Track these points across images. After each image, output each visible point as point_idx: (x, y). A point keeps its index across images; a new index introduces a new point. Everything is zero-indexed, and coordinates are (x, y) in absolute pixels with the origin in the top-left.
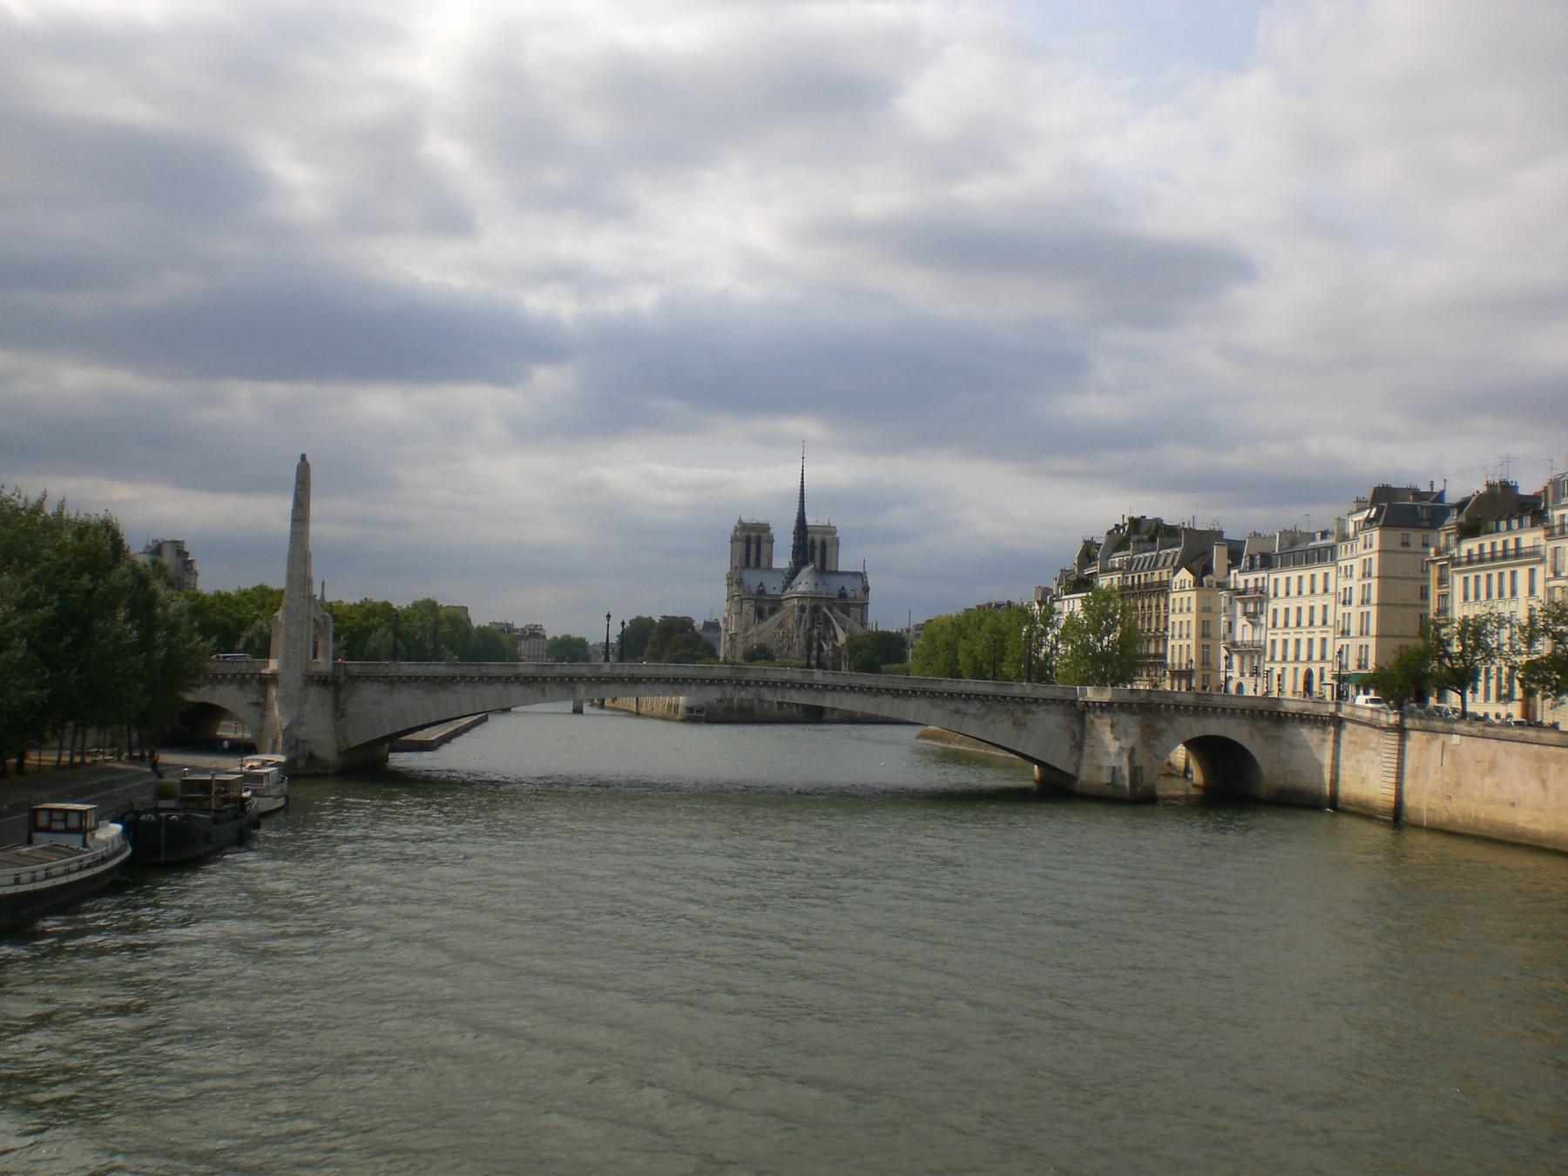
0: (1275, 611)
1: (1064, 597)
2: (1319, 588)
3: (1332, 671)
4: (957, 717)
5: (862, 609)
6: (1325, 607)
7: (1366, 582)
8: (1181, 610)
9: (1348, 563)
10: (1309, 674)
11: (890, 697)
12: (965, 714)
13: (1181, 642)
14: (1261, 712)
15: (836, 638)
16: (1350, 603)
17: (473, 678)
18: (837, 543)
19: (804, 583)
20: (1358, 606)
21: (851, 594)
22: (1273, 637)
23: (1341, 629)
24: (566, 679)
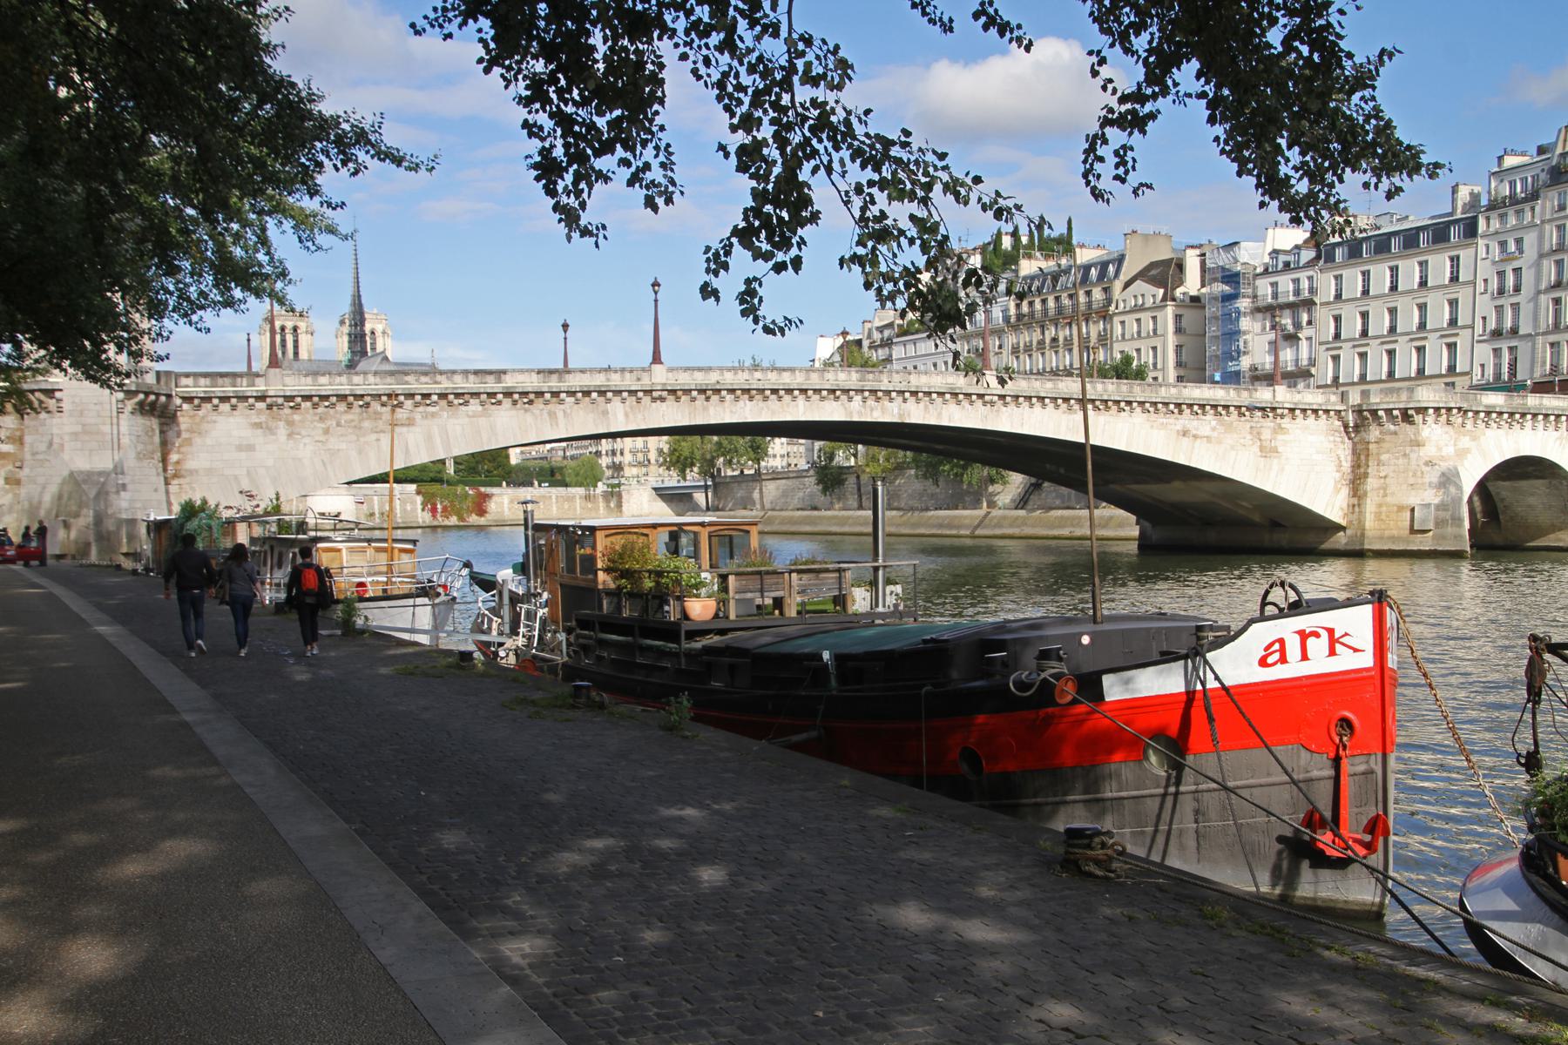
4: (1186, 439)
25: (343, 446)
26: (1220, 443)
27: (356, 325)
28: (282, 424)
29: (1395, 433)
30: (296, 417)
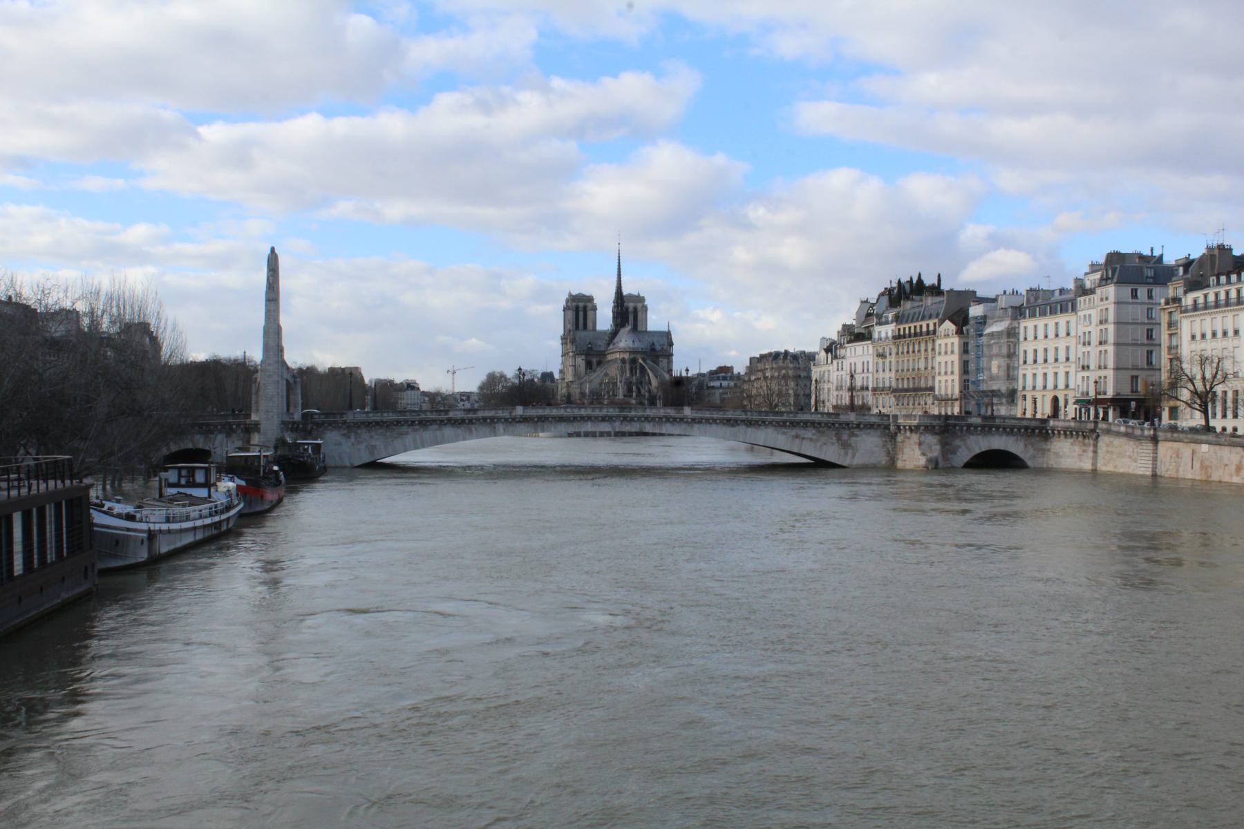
0: (1025, 352)
1: (846, 345)
2: (1062, 333)
3: (1075, 397)
4: (797, 441)
5: (668, 359)
6: (1068, 348)
7: (1103, 327)
8: (946, 353)
9: (1087, 312)
10: (1055, 400)
11: (744, 427)
12: (803, 439)
13: (945, 378)
14: (1033, 430)
15: (650, 383)
16: (1089, 344)
17: (414, 422)
18: (645, 309)
19: (623, 341)
20: (1096, 346)
21: (658, 348)
22: (1024, 372)
23: (1081, 364)
24: (488, 420)
25: (378, 443)
26: (817, 441)
27: (618, 306)
28: (353, 434)
29: (909, 438)
30: (359, 431)
